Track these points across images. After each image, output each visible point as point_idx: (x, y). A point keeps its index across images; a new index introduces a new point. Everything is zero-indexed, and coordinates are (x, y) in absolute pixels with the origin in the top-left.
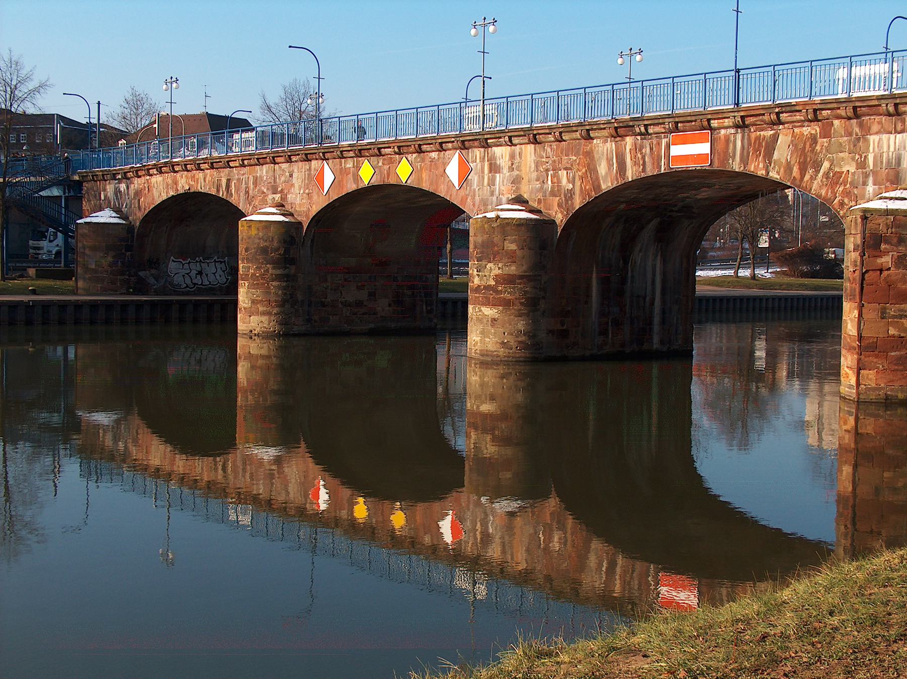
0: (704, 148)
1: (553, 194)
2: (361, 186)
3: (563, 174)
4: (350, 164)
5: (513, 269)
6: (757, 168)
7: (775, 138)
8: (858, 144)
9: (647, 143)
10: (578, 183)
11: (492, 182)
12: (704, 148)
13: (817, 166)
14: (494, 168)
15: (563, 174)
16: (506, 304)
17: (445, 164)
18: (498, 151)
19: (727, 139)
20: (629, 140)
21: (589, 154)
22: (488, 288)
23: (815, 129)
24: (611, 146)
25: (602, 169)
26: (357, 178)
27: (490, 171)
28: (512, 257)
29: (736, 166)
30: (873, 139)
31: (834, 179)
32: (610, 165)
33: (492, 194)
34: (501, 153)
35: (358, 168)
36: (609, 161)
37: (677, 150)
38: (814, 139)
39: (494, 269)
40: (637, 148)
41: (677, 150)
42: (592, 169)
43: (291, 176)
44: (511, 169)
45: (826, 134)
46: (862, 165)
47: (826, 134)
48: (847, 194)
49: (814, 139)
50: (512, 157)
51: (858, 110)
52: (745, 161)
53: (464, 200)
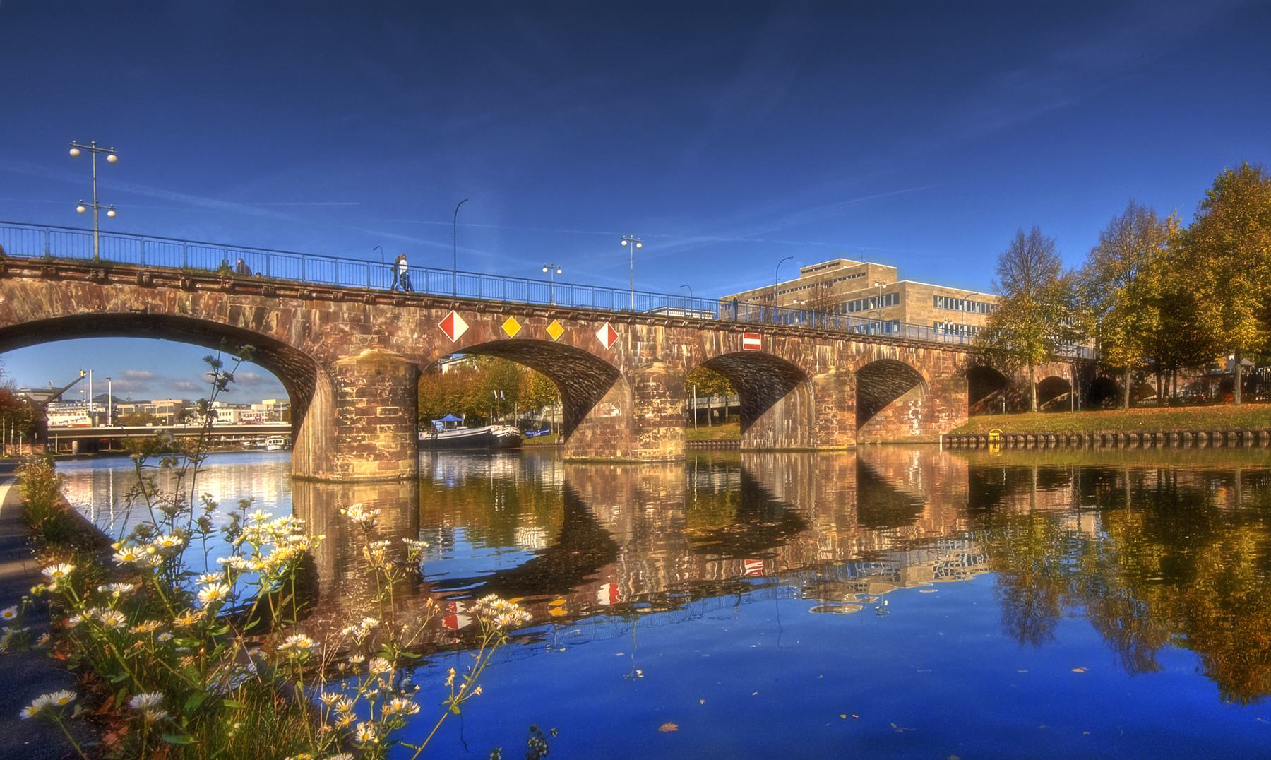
0: (758, 342)
2: (502, 338)
3: (684, 347)
4: (488, 318)
6: (779, 353)
11: (635, 346)
12: (758, 342)
14: (636, 338)
15: (684, 347)
17: (595, 330)
18: (638, 327)
21: (700, 337)
24: (711, 333)
25: (707, 346)
26: (497, 330)
29: (770, 352)
31: (806, 362)
33: (635, 354)
35: (499, 322)
37: (747, 341)
40: (726, 337)
42: (702, 345)
43: (396, 317)
44: (648, 340)
50: (649, 332)
52: (774, 350)
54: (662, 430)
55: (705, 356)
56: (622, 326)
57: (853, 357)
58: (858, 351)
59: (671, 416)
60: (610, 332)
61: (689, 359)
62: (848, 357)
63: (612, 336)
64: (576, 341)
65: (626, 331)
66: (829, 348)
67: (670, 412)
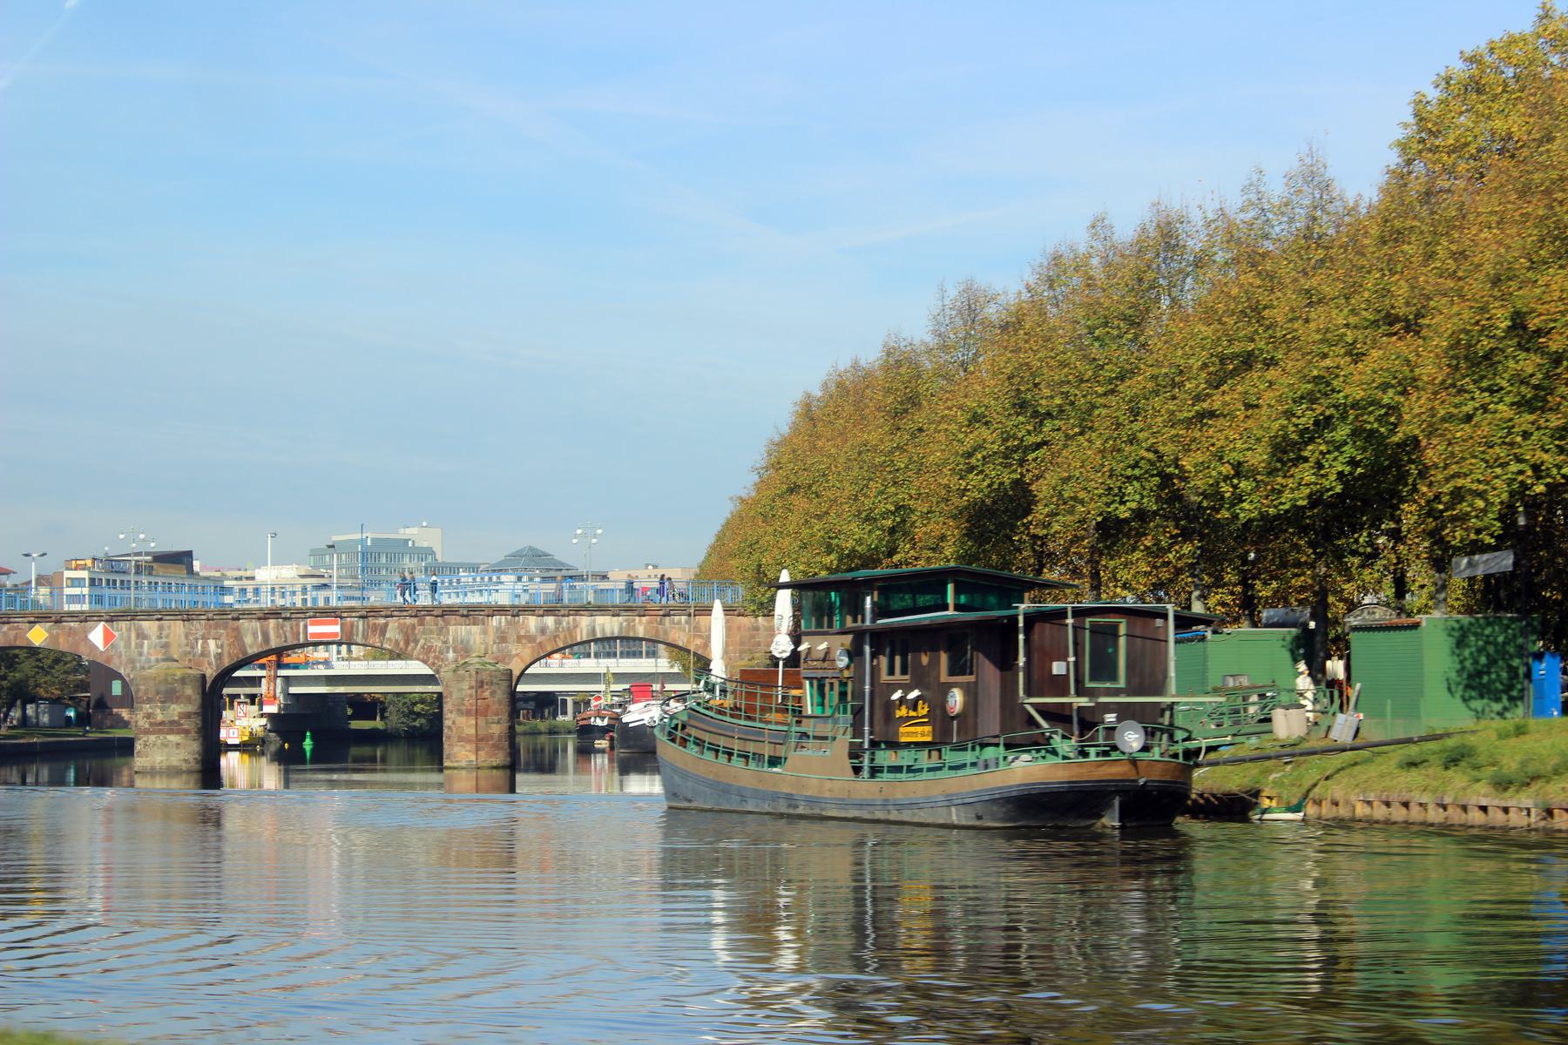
1: (203, 654)
3: (212, 643)
5: (191, 708)
7: (386, 625)
8: (442, 631)
9: (287, 623)
10: (226, 649)
13: (416, 642)
14: (142, 636)
15: (212, 643)
16: (186, 732)
17: (86, 632)
19: (352, 625)
20: (272, 623)
21: (237, 629)
22: (172, 722)
23: (415, 620)
24: (257, 625)
25: (248, 640)
27: (138, 636)
28: (189, 699)
30: (452, 628)
32: (256, 637)
33: (141, 654)
34: (150, 626)
36: (255, 635)
37: (312, 629)
38: (414, 627)
39: (176, 710)
40: (278, 627)
41: (312, 629)
44: (160, 637)
45: (421, 624)
46: (445, 642)
47: (421, 624)
48: (437, 658)
49: (414, 627)
50: (161, 628)
51: (447, 612)
53: (109, 659)
54: (152, 738)
55: (243, 648)
56: (123, 625)
57: (531, 639)
58: (543, 630)
59: (162, 723)
60: (106, 631)
61: (219, 656)
62: (519, 638)
63: (108, 637)
64: (64, 645)
65: (129, 630)
66: (475, 629)
67: (160, 718)
